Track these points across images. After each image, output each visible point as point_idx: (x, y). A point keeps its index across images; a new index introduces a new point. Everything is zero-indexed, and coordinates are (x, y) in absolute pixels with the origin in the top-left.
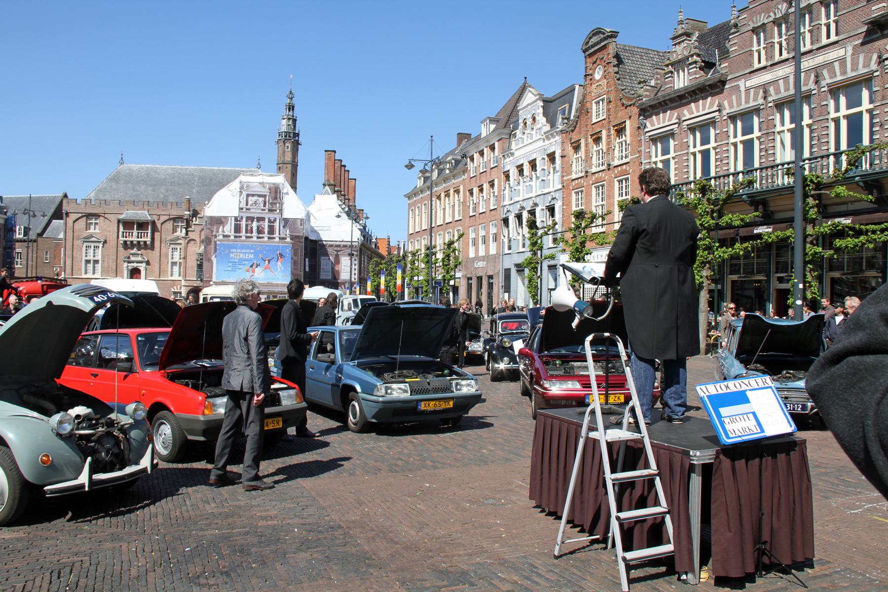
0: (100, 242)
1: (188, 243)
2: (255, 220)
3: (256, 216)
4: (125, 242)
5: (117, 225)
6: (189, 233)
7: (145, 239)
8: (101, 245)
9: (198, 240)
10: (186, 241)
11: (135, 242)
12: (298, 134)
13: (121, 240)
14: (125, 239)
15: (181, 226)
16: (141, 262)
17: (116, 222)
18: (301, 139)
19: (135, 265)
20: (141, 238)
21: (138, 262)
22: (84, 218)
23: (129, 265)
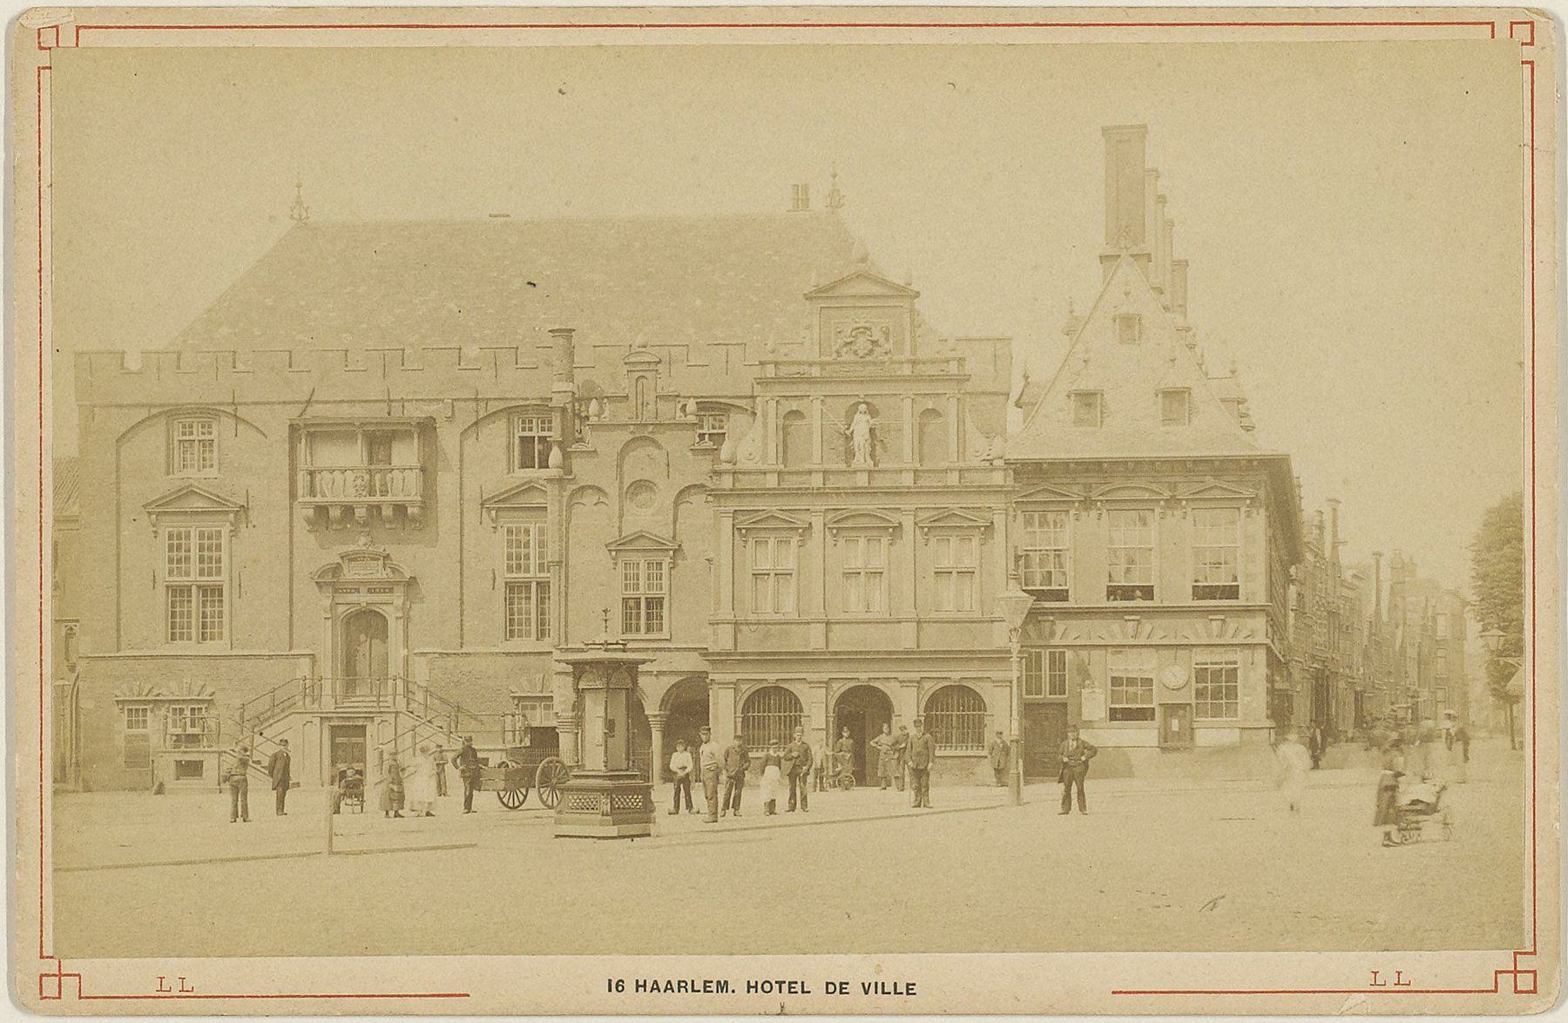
1: (570, 506)
2: (863, 407)
3: (861, 391)
5: (287, 446)
6: (577, 464)
7: (400, 498)
8: (225, 531)
9: (613, 491)
10: (567, 494)
11: (360, 512)
14: (318, 499)
15: (542, 440)
16: (388, 587)
19: (363, 599)
20: (384, 493)
22: (163, 420)
23: (340, 599)
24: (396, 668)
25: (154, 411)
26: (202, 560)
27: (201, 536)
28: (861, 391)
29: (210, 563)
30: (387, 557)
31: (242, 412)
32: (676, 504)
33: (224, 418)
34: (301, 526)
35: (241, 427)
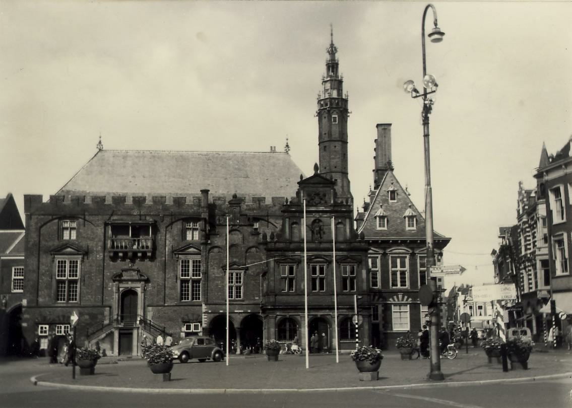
0: (80, 254)
1: (209, 253)
2: (317, 221)
4: (116, 254)
7: (145, 250)
10: (208, 249)
11: (130, 254)
12: (346, 101)
13: (110, 252)
14: (115, 250)
16: (139, 281)
17: (103, 227)
18: (350, 107)
19: (130, 285)
21: (133, 281)
22: (56, 221)
23: (121, 285)
24: (140, 312)
25: (54, 217)
26: (70, 271)
27: (70, 262)
28: (317, 215)
29: (73, 272)
30: (139, 271)
31: (87, 218)
32: (246, 252)
33: (80, 220)
34: (107, 258)
35: (86, 222)
